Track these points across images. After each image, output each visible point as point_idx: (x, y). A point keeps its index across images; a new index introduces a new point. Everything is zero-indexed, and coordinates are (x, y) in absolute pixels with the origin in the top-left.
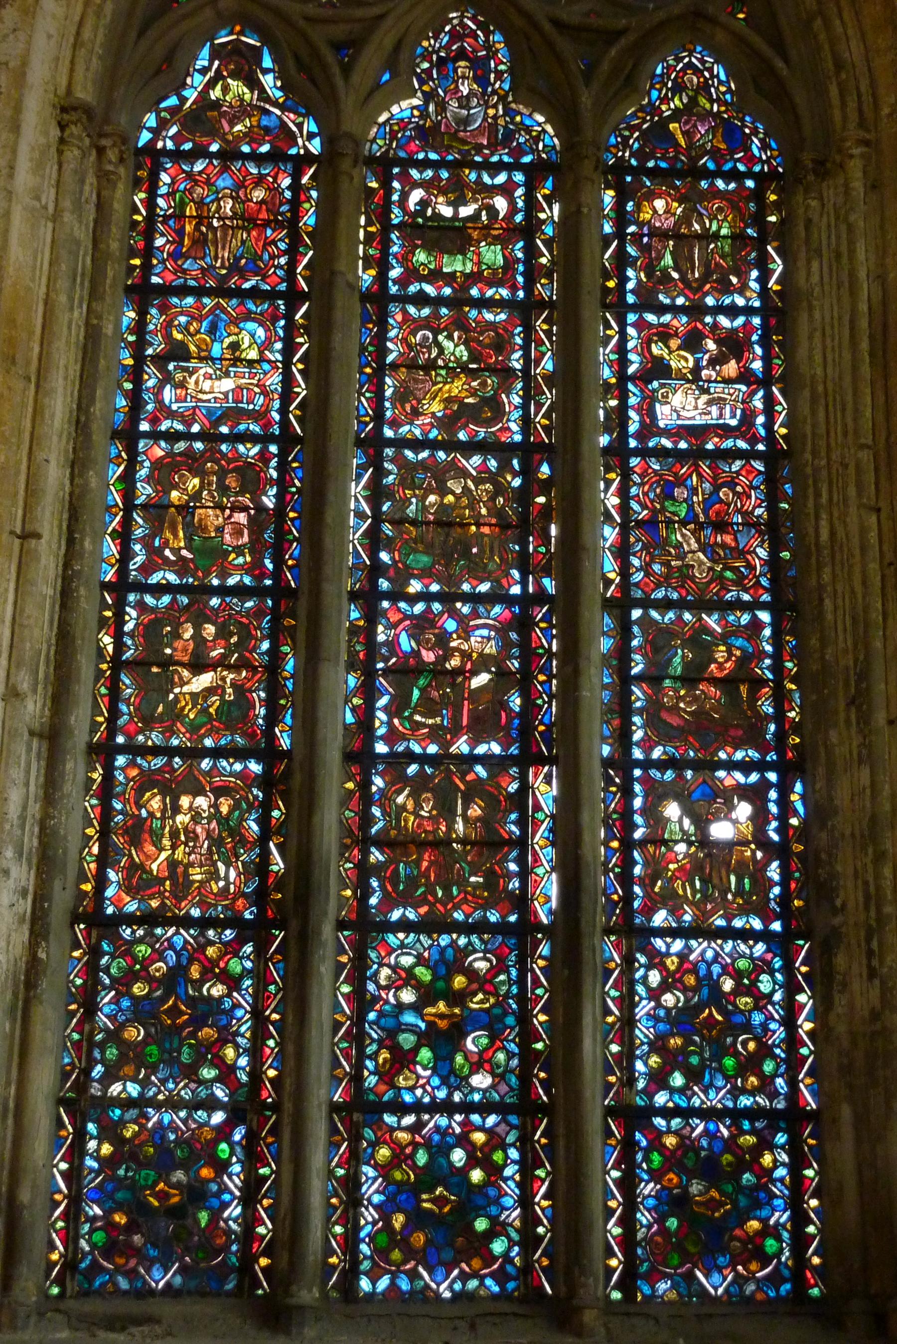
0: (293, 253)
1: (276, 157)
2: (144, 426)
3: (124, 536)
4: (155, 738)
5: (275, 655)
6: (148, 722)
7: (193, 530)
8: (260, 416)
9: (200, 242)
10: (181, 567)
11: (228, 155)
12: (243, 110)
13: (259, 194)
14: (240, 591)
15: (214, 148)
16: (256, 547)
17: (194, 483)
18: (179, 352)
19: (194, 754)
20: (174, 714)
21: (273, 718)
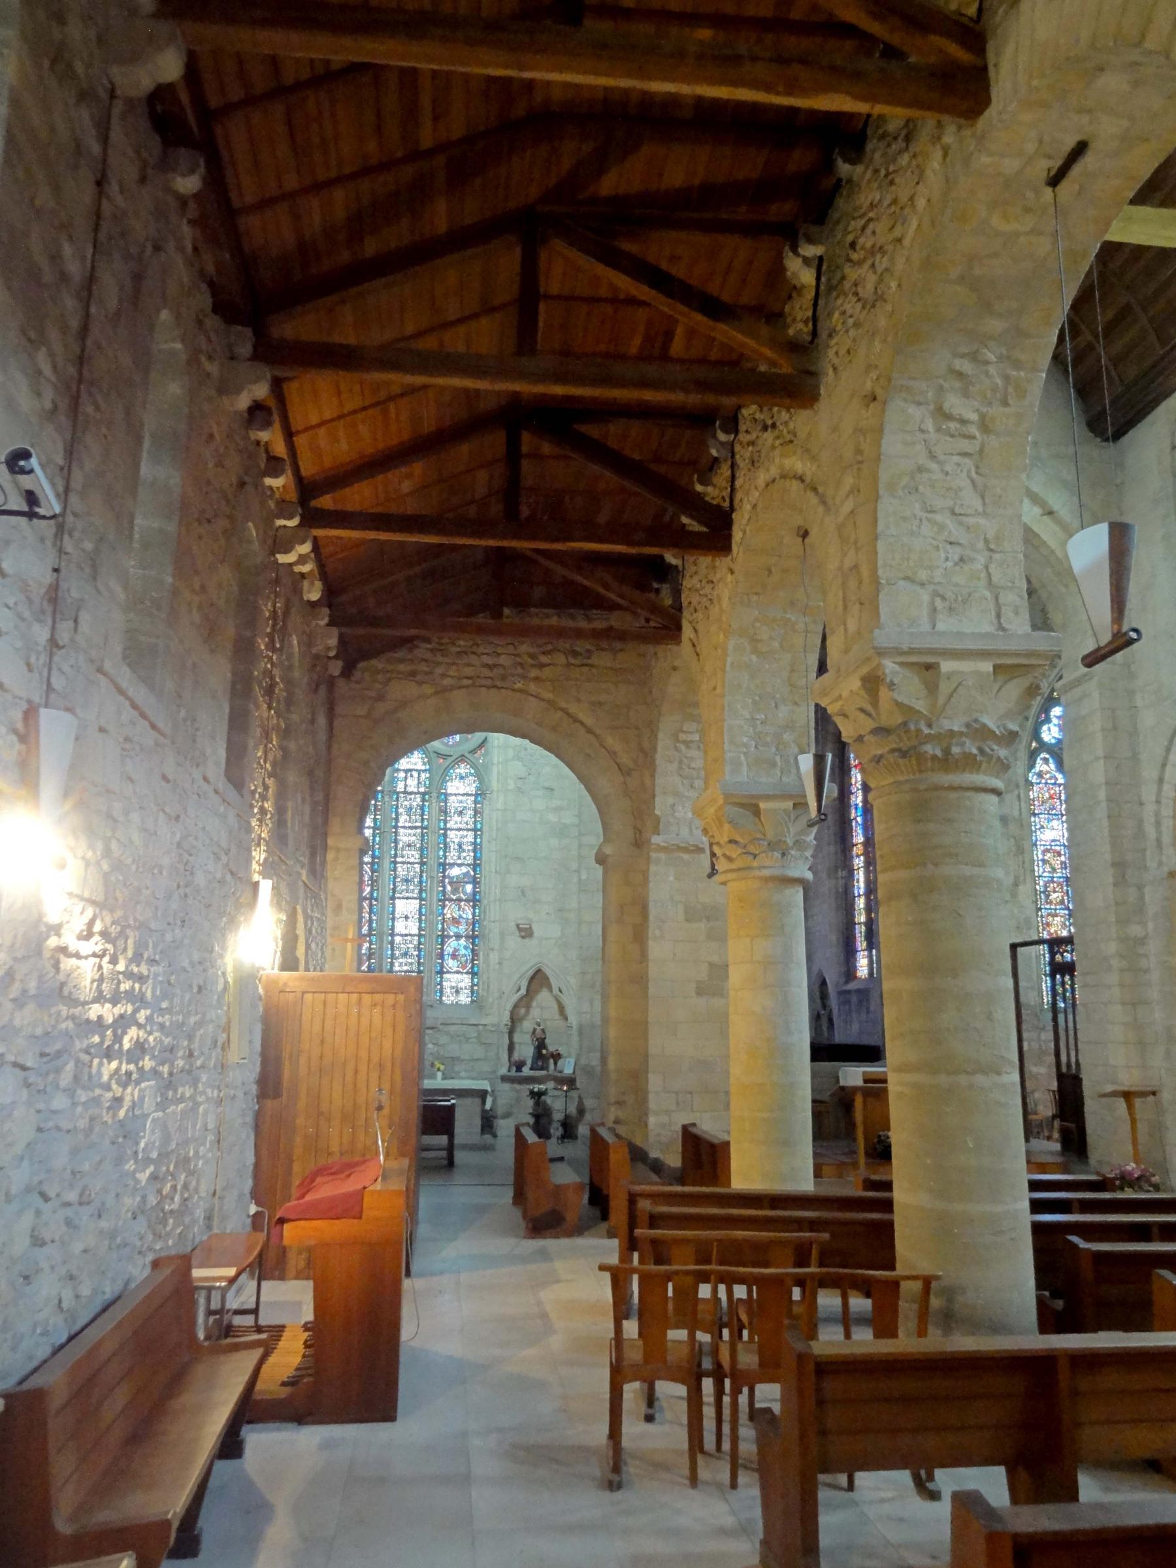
0: (1061, 805)
1: (1055, 784)
2: (1038, 843)
3: (1038, 866)
4: (1048, 906)
5: (1068, 891)
6: (1047, 903)
7: (1050, 864)
8: (1059, 841)
9: (1043, 802)
10: (1049, 872)
11: (1046, 783)
12: (1048, 772)
13: (1052, 792)
14: (1060, 877)
15: (1043, 781)
16: (1062, 868)
17: (1049, 855)
18: (1042, 827)
19: (1056, 909)
20: (1051, 903)
21: (1069, 902)
